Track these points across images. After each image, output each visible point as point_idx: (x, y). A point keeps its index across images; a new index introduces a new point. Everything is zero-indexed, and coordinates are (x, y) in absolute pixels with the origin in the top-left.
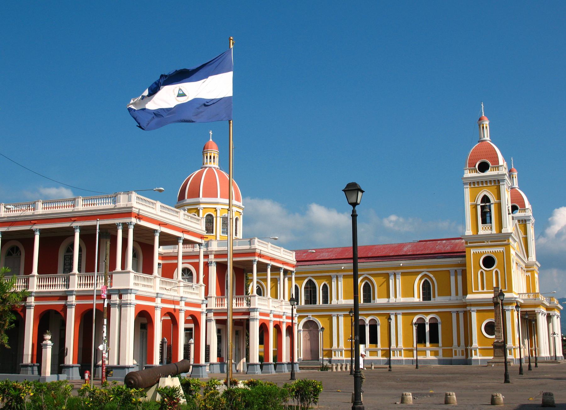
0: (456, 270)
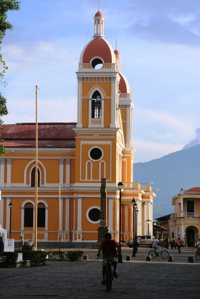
0: (65, 160)
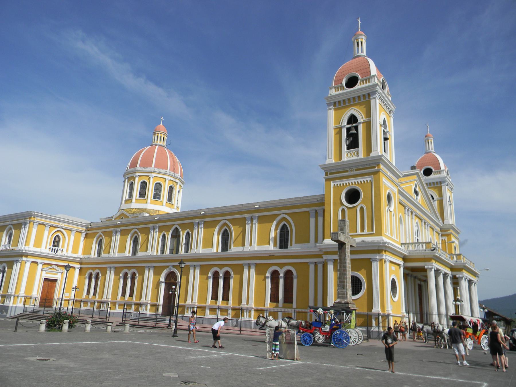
0: (316, 211)
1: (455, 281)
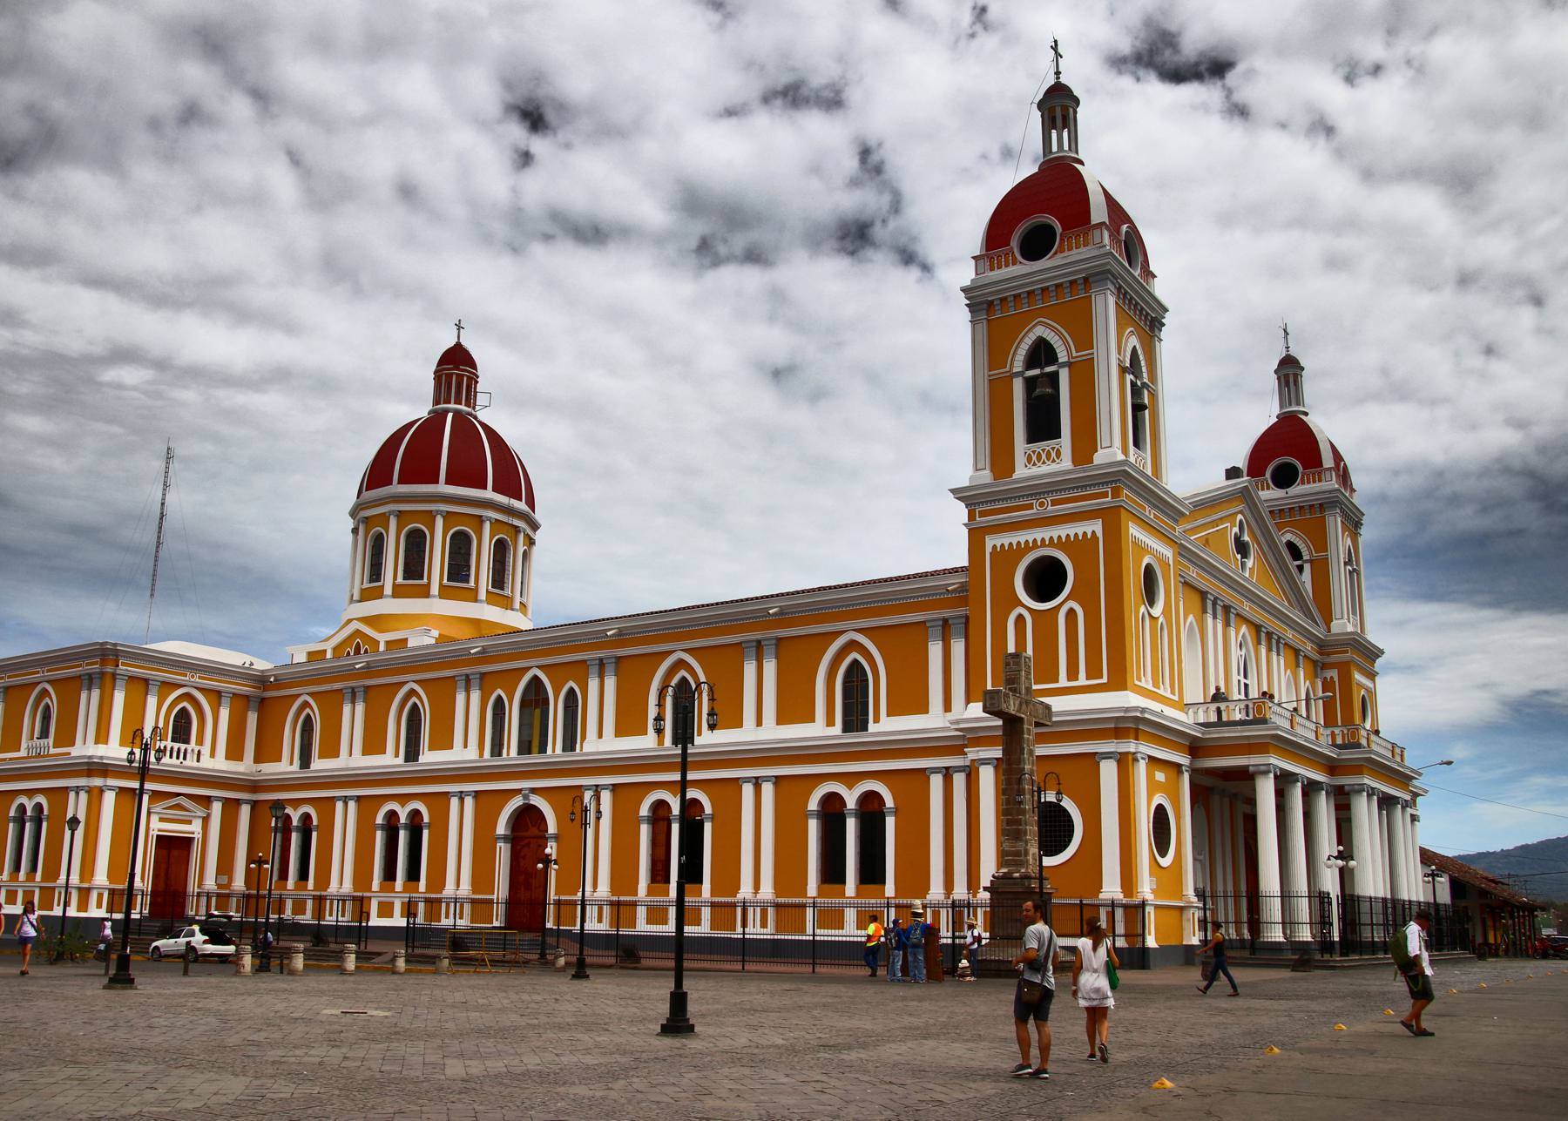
1: (1342, 800)
